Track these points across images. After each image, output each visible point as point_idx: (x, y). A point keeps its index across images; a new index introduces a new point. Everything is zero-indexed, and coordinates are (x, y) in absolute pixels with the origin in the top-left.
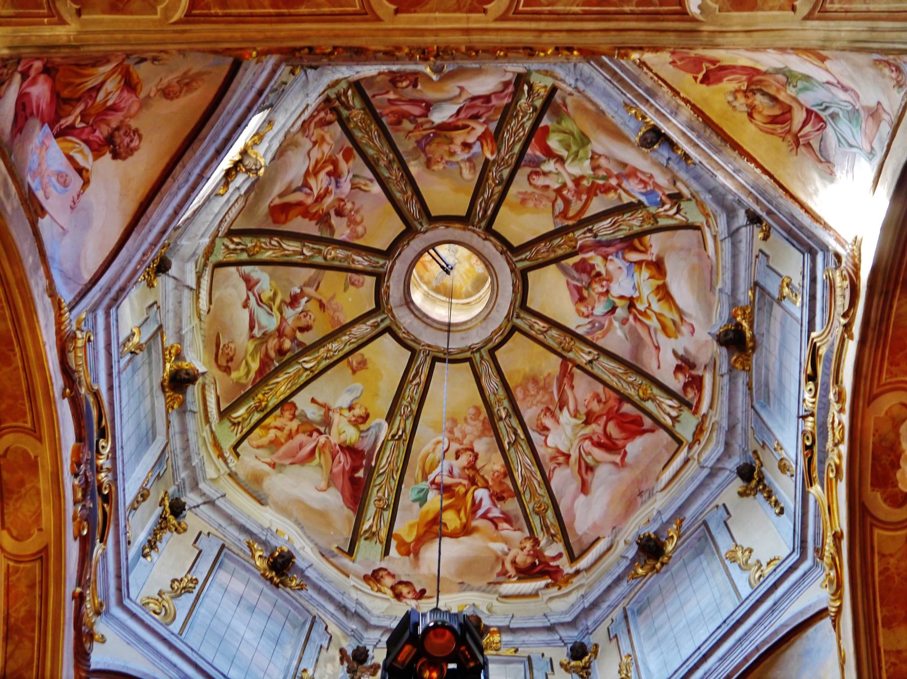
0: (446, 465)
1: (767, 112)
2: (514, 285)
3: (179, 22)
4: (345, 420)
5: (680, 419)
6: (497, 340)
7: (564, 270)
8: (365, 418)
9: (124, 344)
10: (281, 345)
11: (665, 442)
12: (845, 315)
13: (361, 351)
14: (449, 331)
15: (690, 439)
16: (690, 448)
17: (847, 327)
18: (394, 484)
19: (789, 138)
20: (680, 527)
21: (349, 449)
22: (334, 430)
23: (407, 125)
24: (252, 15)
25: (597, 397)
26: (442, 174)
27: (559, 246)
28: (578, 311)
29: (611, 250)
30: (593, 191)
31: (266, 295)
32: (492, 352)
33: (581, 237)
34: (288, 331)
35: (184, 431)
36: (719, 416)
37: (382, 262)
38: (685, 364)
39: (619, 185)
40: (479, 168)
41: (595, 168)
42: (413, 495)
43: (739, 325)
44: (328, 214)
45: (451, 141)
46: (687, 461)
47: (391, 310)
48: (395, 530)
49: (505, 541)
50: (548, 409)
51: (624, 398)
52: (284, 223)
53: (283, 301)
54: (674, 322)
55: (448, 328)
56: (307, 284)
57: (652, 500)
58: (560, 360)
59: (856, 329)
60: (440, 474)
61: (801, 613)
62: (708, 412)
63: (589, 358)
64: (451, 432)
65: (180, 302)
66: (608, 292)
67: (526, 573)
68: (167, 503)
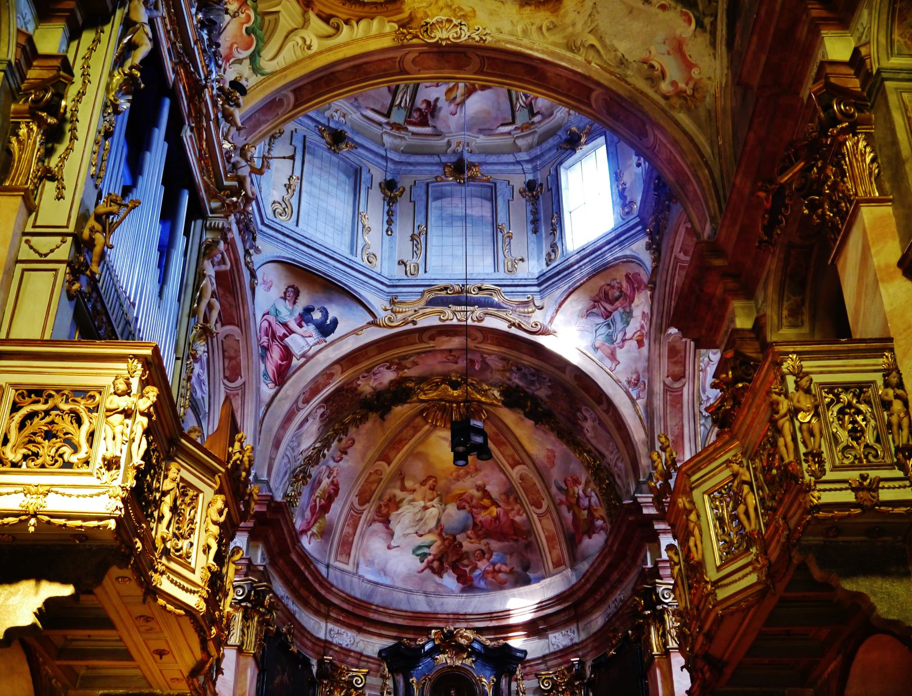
1: (610, 292)
11: (385, 103)
15: (391, 122)
16: (387, 123)
17: (514, 324)
19: (597, 298)
20: (352, 147)
38: (432, 108)
46: (380, 124)
54: (455, 98)
59: (513, 330)
61: (368, 302)
62: (410, 132)
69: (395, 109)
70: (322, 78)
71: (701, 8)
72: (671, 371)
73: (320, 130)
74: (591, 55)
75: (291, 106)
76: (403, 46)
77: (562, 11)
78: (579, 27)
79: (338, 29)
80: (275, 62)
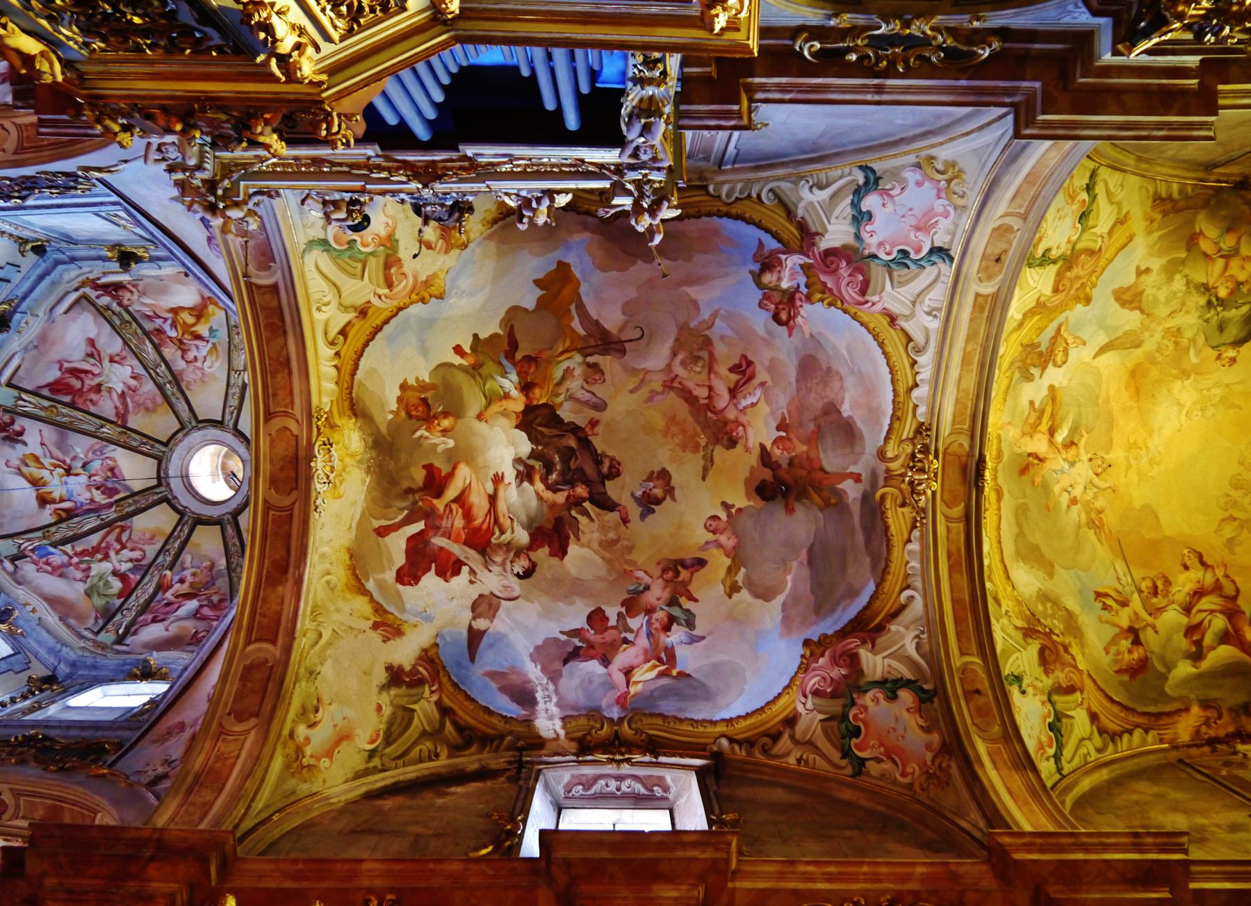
6: (180, 435)
7: (127, 488)
23: (215, 599)
26: (205, 557)
27: (130, 505)
29: (86, 507)
30: (96, 549)
33: (111, 514)
39: (71, 557)
40: (178, 563)
41: (89, 569)
42: (218, 333)
45: (192, 585)
49: (144, 304)
51: (71, 405)
54: (27, 465)
58: (129, 425)
60: (204, 349)
67: (118, 286)
69: (15, 393)
70: (282, 319)
71: (388, 750)
73: (12, 300)
74: (312, 636)
75: (254, 280)
76: (310, 416)
77: (349, 596)
78: (336, 617)
79: (332, 343)
80: (314, 269)
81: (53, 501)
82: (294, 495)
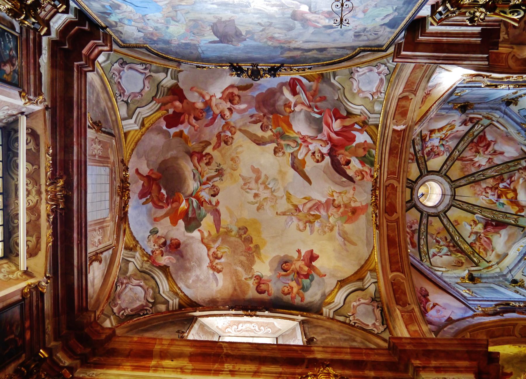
0: (491, 197)
2: (432, 175)
3: (405, 275)
4: (475, 228)
5: (482, 124)
6: (448, 180)
7: (429, 160)
8: (474, 221)
9: (472, 295)
10: (452, 246)
12: (484, 78)
13: (452, 222)
14: (445, 195)
16: (493, 121)
17: (487, 77)
18: (497, 213)
19: (427, 96)
20: (524, 124)
21: (485, 227)
22: (479, 231)
24: (400, 254)
25: (470, 150)
28: (442, 155)
29: (424, 146)
31: (437, 250)
32: (452, 182)
34: (447, 244)
35: (487, 278)
36: (484, 113)
37: (424, 215)
38: (464, 123)
43: (459, 107)
44: (412, 231)
46: (498, 122)
47: (439, 212)
48: (514, 213)
49: (519, 178)
50: (473, 165)
51: (472, 141)
52: (415, 244)
53: (438, 245)
54: (450, 126)
55: (443, 195)
56: (432, 237)
57: (510, 132)
60: (494, 198)
63: (457, 152)
64: (479, 195)
65: (447, 277)
66: (437, 146)
68: (514, 285)
72: (408, 102)
81: (431, 134)
82: (520, 336)
